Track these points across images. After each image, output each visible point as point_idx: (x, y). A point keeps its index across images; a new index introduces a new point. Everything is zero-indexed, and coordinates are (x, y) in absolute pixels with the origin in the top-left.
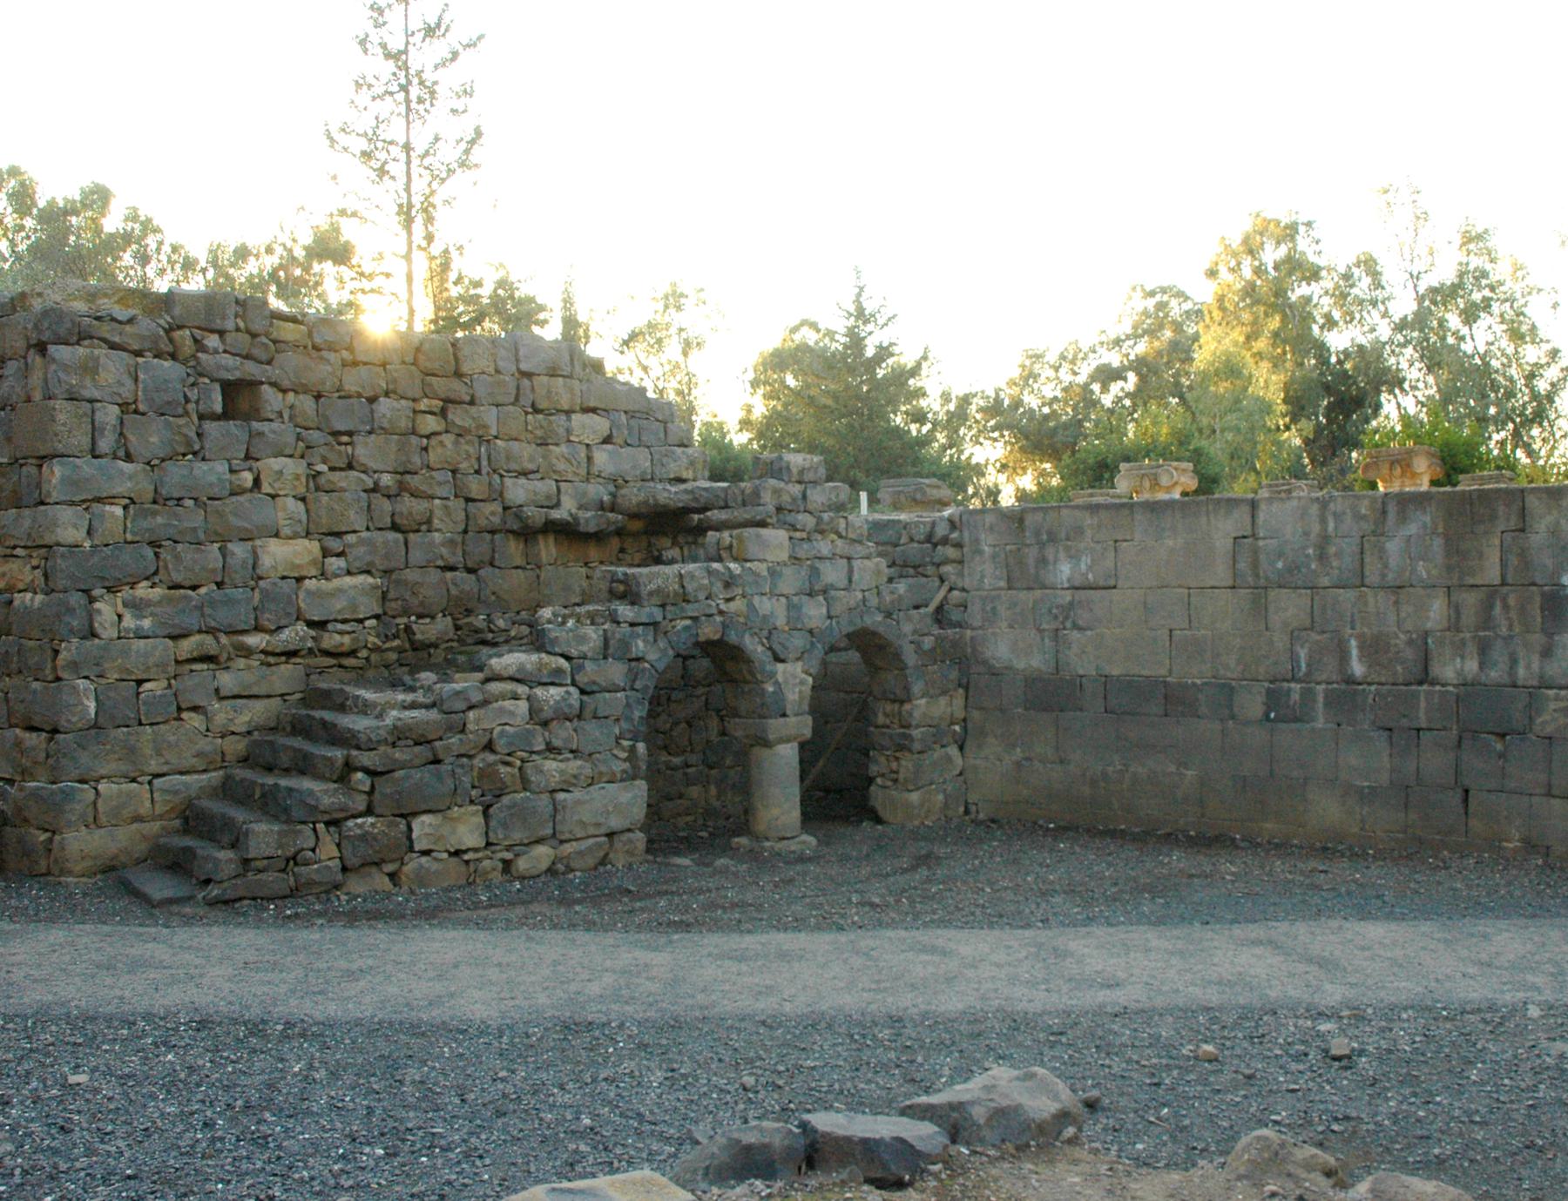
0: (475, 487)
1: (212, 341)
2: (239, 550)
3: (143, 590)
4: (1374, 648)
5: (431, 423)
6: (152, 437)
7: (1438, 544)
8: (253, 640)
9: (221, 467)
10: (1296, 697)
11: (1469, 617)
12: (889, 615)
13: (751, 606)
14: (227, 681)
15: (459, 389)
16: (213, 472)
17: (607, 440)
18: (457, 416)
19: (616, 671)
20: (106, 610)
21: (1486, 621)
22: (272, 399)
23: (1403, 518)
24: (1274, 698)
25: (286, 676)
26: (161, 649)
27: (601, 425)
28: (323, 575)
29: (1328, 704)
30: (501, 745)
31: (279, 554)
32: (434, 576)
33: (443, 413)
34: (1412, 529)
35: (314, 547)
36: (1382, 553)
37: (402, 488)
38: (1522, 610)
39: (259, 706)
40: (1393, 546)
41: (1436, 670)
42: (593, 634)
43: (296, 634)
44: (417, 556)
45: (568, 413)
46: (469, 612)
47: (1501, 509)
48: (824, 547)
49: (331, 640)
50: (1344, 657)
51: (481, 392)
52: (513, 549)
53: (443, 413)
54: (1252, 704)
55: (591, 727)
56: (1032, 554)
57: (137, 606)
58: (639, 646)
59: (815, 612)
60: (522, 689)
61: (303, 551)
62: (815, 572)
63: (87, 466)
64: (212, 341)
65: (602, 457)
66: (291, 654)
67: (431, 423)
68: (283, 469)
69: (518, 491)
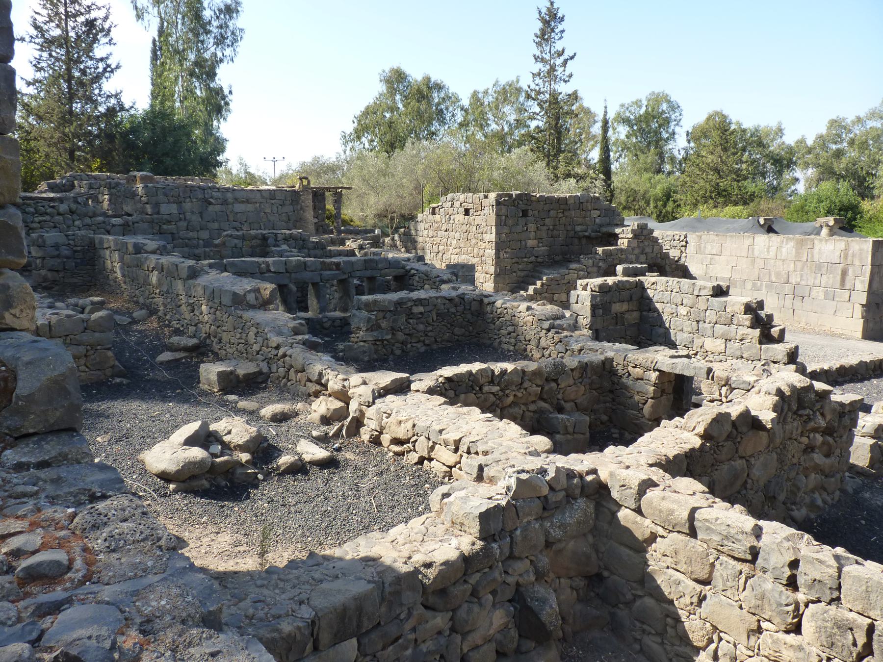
0: (569, 228)
1: (521, 202)
2: (523, 243)
4: (778, 274)
6: (510, 222)
7: (794, 250)
8: (525, 260)
10: (759, 285)
11: (798, 269)
12: (663, 259)
13: (627, 257)
16: (519, 228)
18: (566, 213)
21: (802, 269)
22: (530, 212)
23: (787, 244)
24: (754, 285)
25: (530, 266)
26: (509, 260)
27: (598, 212)
28: (538, 247)
29: (766, 287)
30: (571, 282)
31: (531, 243)
33: (563, 213)
34: (789, 246)
36: (781, 252)
37: (554, 229)
38: (811, 268)
39: (525, 272)
40: (784, 250)
41: (790, 281)
42: (590, 261)
43: (532, 259)
45: (590, 211)
46: (566, 255)
47: (809, 243)
48: (646, 243)
49: (539, 260)
50: (770, 275)
51: (571, 207)
53: (563, 213)
54: (749, 285)
56: (703, 245)
57: (506, 252)
58: (601, 264)
60: (576, 272)
61: (535, 242)
62: (643, 250)
64: (521, 202)
65: (597, 220)
67: (561, 215)
68: (532, 227)
69: (578, 228)
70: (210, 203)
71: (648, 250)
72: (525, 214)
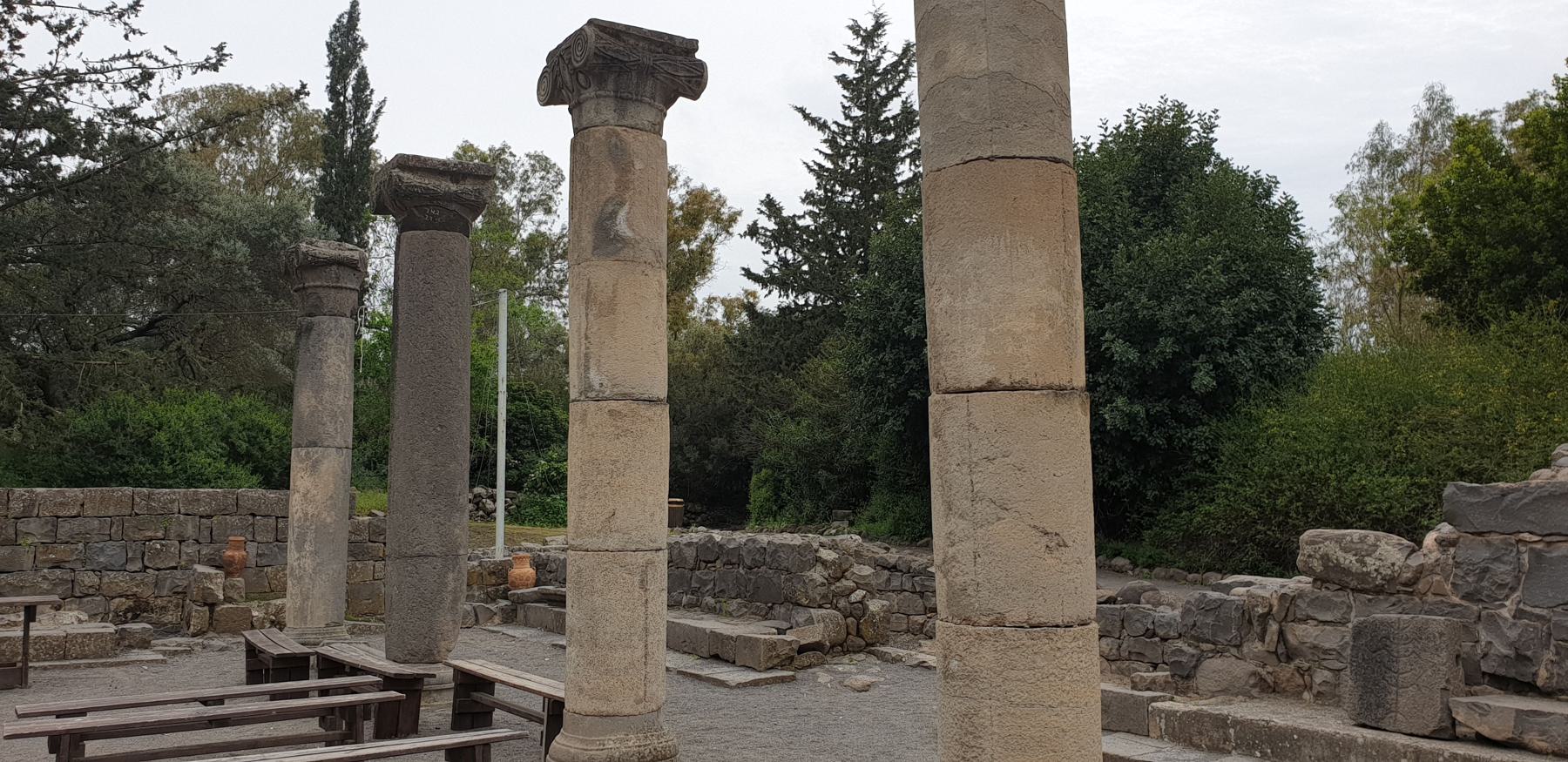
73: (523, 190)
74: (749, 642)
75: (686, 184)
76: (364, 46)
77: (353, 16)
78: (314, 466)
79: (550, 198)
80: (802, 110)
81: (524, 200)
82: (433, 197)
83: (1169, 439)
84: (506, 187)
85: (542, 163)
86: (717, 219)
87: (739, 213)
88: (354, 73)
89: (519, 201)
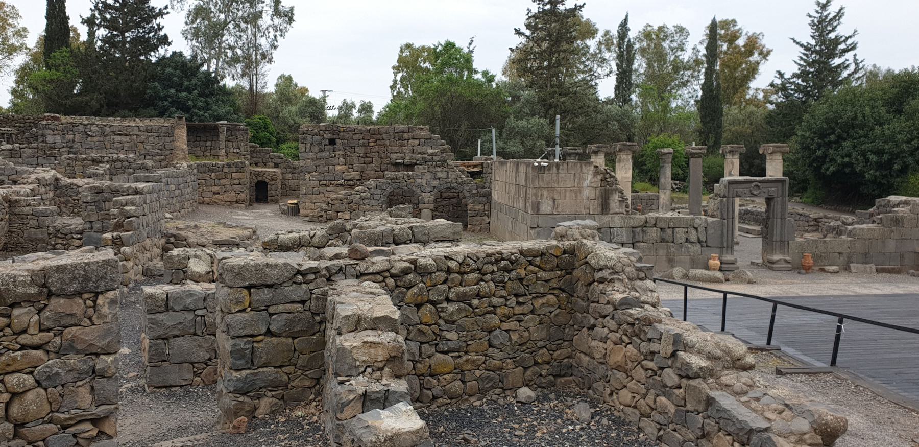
2: (331, 167)
3: (314, 173)
5: (373, 144)
9: (328, 153)
14: (329, 189)
15: (379, 136)
17: (419, 145)
18: (378, 142)
19: (379, 191)
20: (307, 176)
27: (417, 142)
32: (372, 172)
35: (347, 167)
44: (368, 169)
52: (393, 168)
55: (373, 201)
59: (436, 183)
63: (305, 154)
66: (341, 185)
67: (373, 144)
70: (89, 135)
71: (440, 175)
72: (332, 142)
73: (671, 41)
74: (755, 230)
75: (746, 34)
76: (629, 30)
77: (626, 20)
78: (665, 193)
79: (684, 44)
80: (793, 39)
81: (672, 45)
82: (697, 153)
83: (888, 182)
84: (664, 40)
85: (681, 30)
86: (761, 53)
87: (772, 50)
88: (626, 40)
89: (670, 47)
